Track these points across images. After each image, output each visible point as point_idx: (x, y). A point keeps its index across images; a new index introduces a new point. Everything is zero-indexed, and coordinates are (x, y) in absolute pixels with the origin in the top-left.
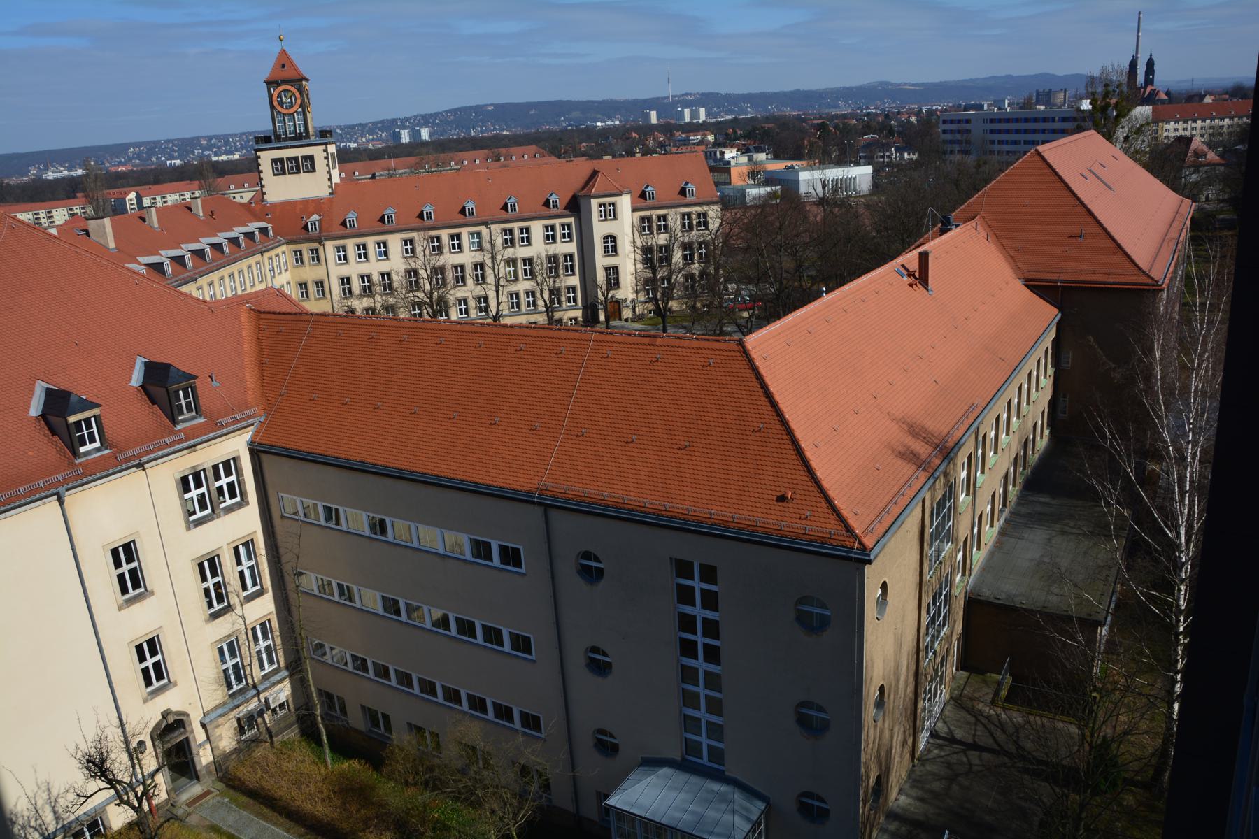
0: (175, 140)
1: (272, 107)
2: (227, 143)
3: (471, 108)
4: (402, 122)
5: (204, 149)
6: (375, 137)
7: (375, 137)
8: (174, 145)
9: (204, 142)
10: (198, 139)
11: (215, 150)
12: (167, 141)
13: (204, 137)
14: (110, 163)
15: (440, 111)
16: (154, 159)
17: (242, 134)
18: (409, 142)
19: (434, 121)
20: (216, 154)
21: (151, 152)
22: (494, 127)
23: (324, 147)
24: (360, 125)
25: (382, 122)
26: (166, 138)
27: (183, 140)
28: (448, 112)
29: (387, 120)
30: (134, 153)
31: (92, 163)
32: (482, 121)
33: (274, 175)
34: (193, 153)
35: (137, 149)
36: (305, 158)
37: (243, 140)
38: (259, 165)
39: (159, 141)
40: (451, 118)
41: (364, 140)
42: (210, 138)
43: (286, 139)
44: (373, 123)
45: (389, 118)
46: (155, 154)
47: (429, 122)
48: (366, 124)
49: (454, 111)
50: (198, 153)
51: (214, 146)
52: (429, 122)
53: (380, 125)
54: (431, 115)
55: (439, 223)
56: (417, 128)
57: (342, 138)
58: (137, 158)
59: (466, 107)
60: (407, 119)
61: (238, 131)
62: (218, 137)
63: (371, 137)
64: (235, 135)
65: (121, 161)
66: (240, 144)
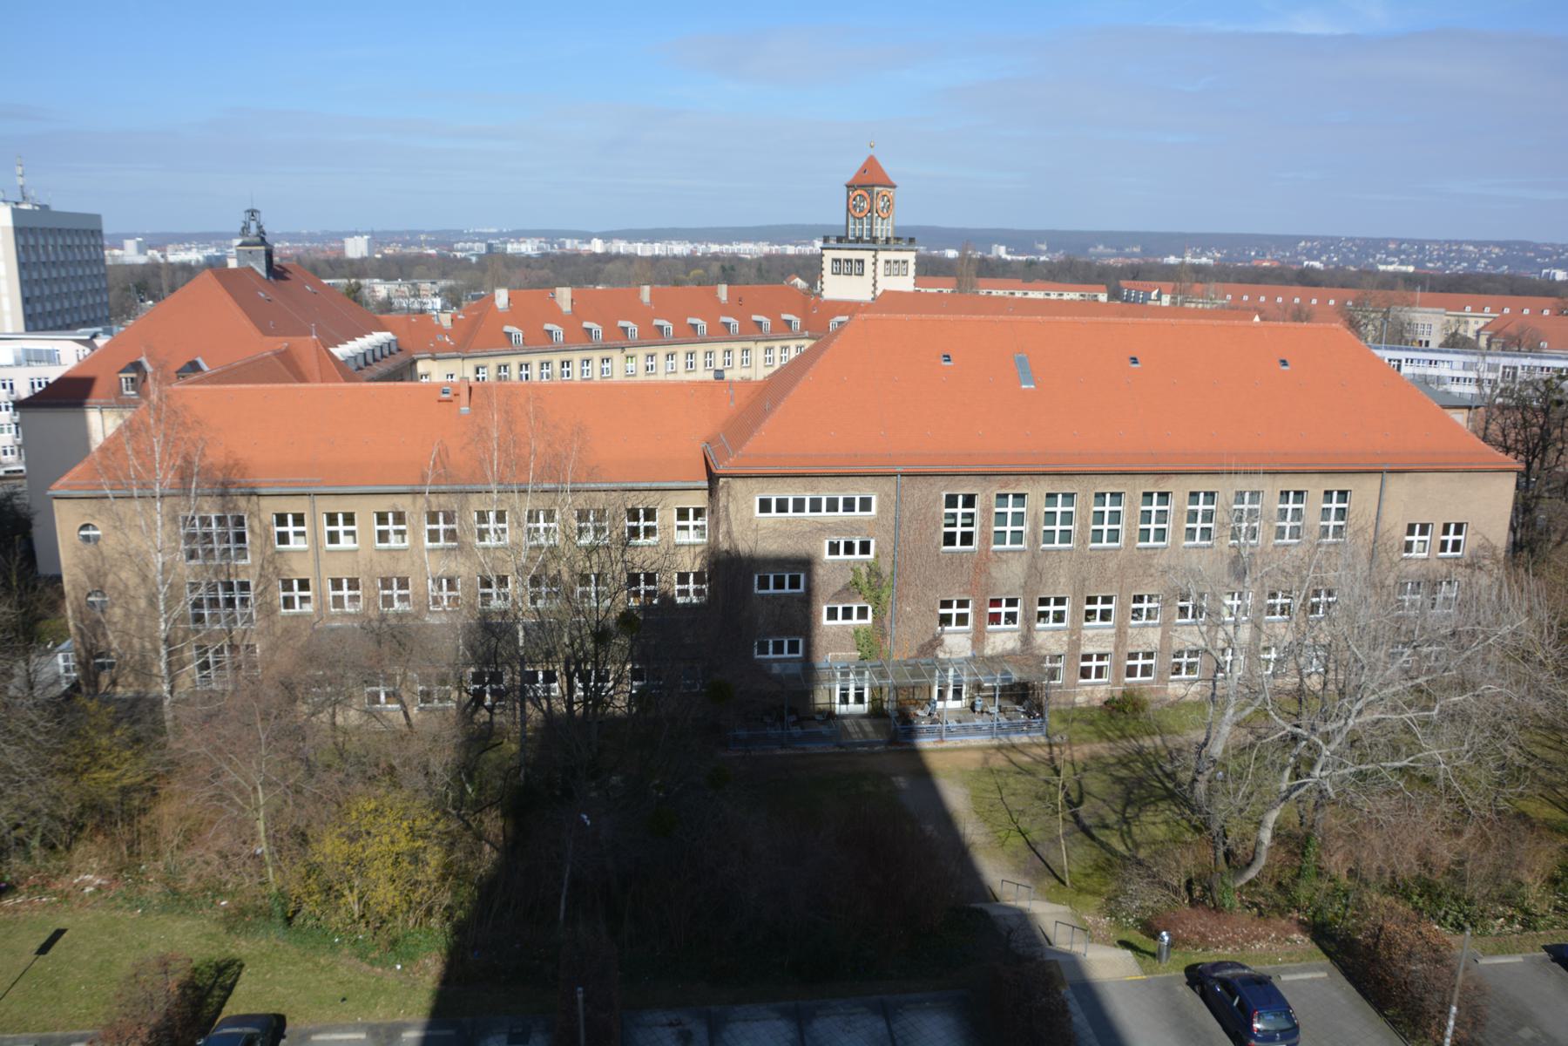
2: (1421, 250)
8: (1354, 245)
10: (1387, 241)
11: (1403, 257)
12: (1348, 240)
13: (1394, 240)
14: (1272, 255)
17: (1446, 242)
26: (1349, 236)
27: (1366, 240)
30: (1304, 248)
34: (1374, 257)
35: (1309, 244)
37: (1443, 250)
39: (1339, 239)
42: (1402, 242)
51: (1404, 252)
61: (1442, 237)
62: (1411, 242)
64: (1436, 242)
66: (1438, 255)
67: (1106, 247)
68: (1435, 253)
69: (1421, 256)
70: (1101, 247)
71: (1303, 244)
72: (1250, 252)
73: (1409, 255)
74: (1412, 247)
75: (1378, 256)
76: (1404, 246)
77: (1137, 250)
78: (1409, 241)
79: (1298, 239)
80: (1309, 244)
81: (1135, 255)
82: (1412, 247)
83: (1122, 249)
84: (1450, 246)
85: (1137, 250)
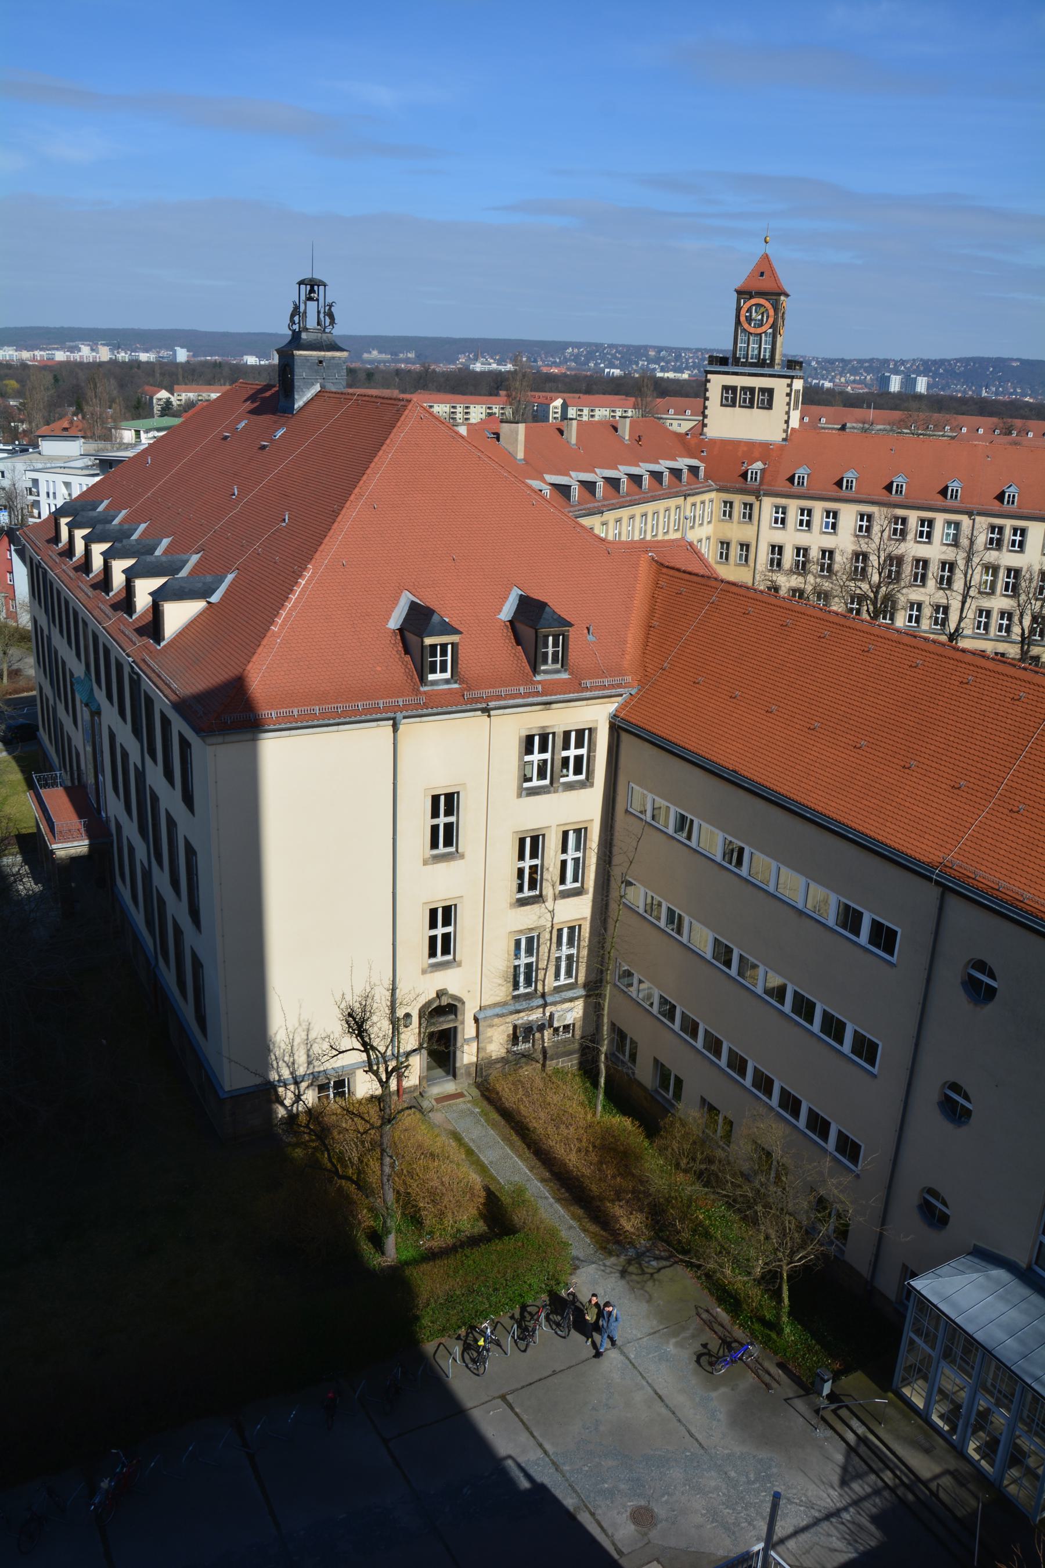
0: (621, 346)
1: (738, 322)
2: (678, 357)
3: (989, 360)
4: (895, 365)
5: (650, 361)
6: (858, 378)
7: (858, 378)
9: (652, 353)
10: (646, 348)
11: (662, 364)
12: (611, 346)
13: (654, 347)
14: (543, 362)
15: (948, 357)
16: (592, 365)
17: (698, 350)
18: (899, 392)
19: (937, 370)
20: (663, 370)
21: (590, 356)
22: (1015, 391)
23: (789, 381)
24: (842, 360)
25: (871, 361)
27: (628, 347)
28: (958, 360)
29: (878, 360)
30: (572, 354)
31: (524, 359)
32: (1000, 379)
33: (722, 405)
34: (637, 364)
35: (576, 350)
36: (763, 390)
38: (706, 390)
39: (602, 345)
40: (960, 368)
41: (843, 380)
42: (660, 349)
43: (744, 365)
44: (860, 361)
45: (881, 357)
46: (594, 358)
47: (930, 371)
48: (850, 361)
49: (966, 361)
50: (643, 365)
51: (663, 359)
52: (930, 371)
53: (867, 364)
54: (935, 362)
55: (1025, 511)
56: (913, 376)
57: (816, 374)
58: (573, 360)
59: (983, 358)
60: (903, 362)
62: (669, 350)
63: (852, 378)
64: (688, 350)
65: (555, 362)
67: (380, 352)
68: (690, 361)
69: (678, 364)
70: (375, 353)
71: (570, 350)
72: (522, 357)
73: (668, 362)
74: (670, 355)
75: (641, 363)
76: (663, 353)
77: (411, 355)
78: (667, 349)
79: (566, 345)
80: (576, 350)
81: (408, 361)
82: (670, 355)
83: (396, 355)
84: (702, 354)
85: (411, 355)
